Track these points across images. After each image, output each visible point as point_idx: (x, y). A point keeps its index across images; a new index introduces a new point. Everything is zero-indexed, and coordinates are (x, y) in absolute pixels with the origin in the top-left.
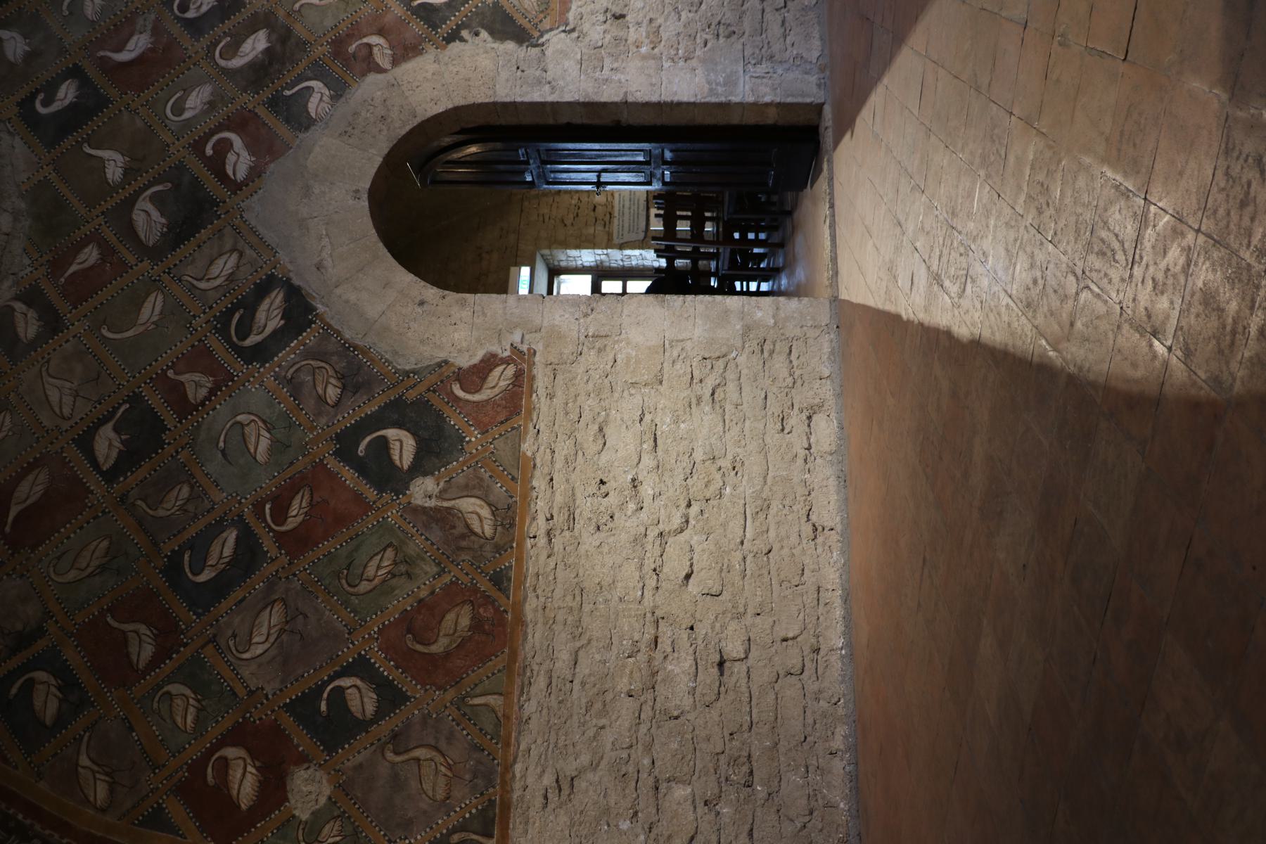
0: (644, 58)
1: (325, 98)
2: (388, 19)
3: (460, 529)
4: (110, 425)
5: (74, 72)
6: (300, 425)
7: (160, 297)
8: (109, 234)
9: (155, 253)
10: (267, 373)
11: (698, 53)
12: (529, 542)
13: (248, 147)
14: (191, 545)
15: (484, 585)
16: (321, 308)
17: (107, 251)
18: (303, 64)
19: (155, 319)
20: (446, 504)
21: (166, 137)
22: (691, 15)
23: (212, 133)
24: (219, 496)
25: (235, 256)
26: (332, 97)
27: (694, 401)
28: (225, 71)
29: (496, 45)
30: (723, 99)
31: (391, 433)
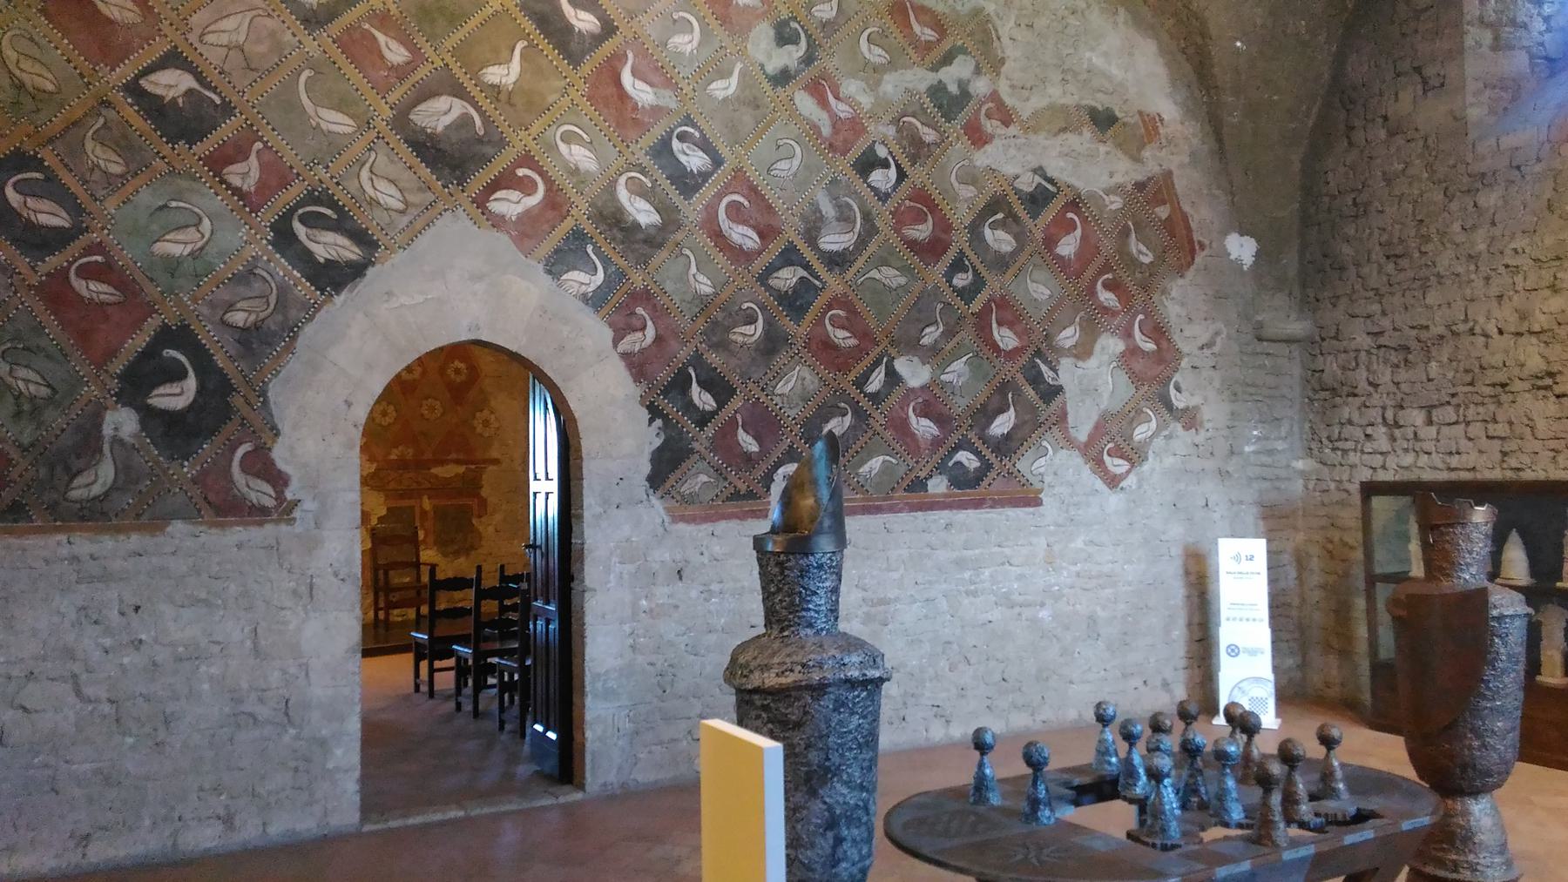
0: (635, 605)
3: (76, 464)
4: (195, 85)
5: (609, 29)
6: (198, 286)
7: (349, 130)
8: (423, 72)
9: (401, 121)
10: (260, 247)
11: (640, 659)
12: (62, 538)
13: (528, 212)
14: (51, 178)
16: (339, 300)
17: (402, 72)
18: (622, 262)
19: (324, 126)
20: (106, 448)
21: (536, 128)
22: (683, 647)
23: (542, 174)
24: (111, 206)
25: (397, 204)
26: (585, 295)
28: (613, 184)
30: (588, 689)
31: (191, 383)
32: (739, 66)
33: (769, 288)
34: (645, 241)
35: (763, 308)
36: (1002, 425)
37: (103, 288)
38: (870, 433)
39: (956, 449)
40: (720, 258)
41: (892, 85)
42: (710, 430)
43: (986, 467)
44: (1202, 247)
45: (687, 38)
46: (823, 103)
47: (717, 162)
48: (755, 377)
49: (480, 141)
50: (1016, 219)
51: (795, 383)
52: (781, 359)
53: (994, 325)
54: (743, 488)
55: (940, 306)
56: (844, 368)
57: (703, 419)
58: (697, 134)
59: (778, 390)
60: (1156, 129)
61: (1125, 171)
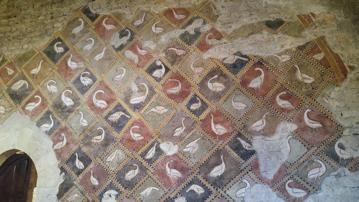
1: (47, 129)
2: (72, 145)
5: (66, 49)
8: (16, 75)
9: (9, 90)
13: (36, 108)
17: (11, 77)
18: (59, 119)
23: (41, 96)
26: (46, 131)
28: (61, 94)
29: (58, 186)
32: (105, 48)
33: (108, 121)
34: (68, 111)
35: (105, 129)
36: (217, 172)
38: (147, 176)
39: (191, 184)
40: (92, 113)
41: (164, 39)
42: (81, 177)
43: (208, 193)
44: (352, 68)
45: (90, 45)
46: (136, 52)
47: (94, 80)
48: (100, 155)
49: (27, 90)
50: (225, 76)
51: (115, 157)
52: (111, 147)
53: (212, 124)
55: (183, 119)
56: (136, 149)
57: (79, 172)
58: (89, 73)
59: (108, 160)
60: (310, 20)
61: (291, 43)
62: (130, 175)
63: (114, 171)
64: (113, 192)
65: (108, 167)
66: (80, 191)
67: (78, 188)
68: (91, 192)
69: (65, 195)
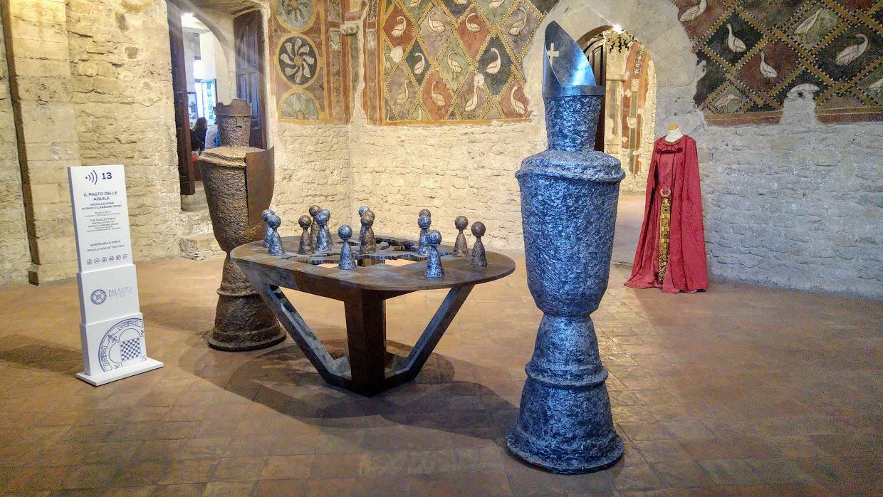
2: (718, 10)
3: (467, 97)
15: (451, 109)
27: (510, 192)
29: (695, 84)
31: (499, 61)
37: (475, 26)
42: (739, 65)
54: (761, 103)
57: (735, 58)
59: (798, 31)
62: (847, 55)
63: (811, 50)
64: (808, 88)
65: (799, 44)
66: (739, 89)
67: (734, 85)
68: (760, 91)
69: (710, 97)
